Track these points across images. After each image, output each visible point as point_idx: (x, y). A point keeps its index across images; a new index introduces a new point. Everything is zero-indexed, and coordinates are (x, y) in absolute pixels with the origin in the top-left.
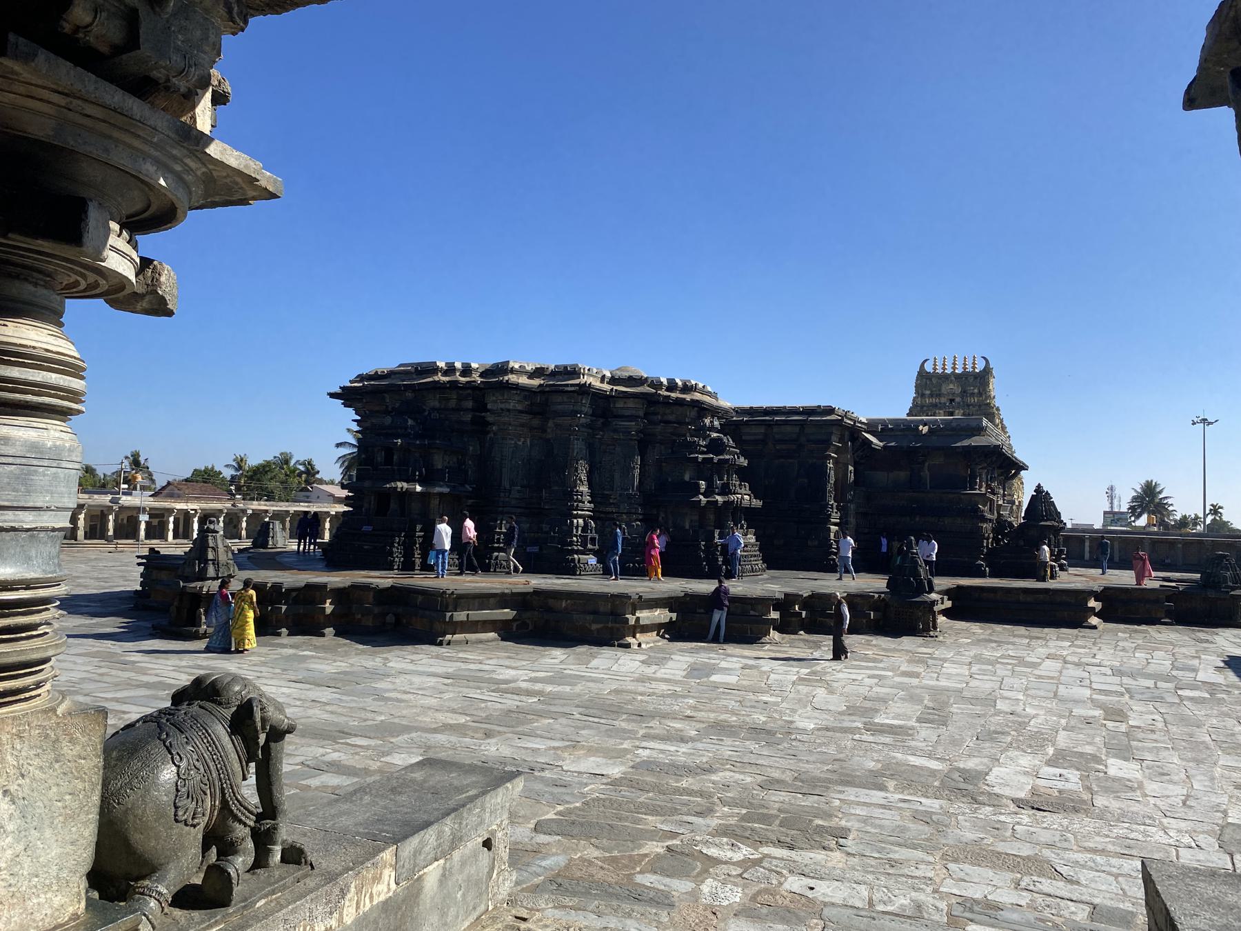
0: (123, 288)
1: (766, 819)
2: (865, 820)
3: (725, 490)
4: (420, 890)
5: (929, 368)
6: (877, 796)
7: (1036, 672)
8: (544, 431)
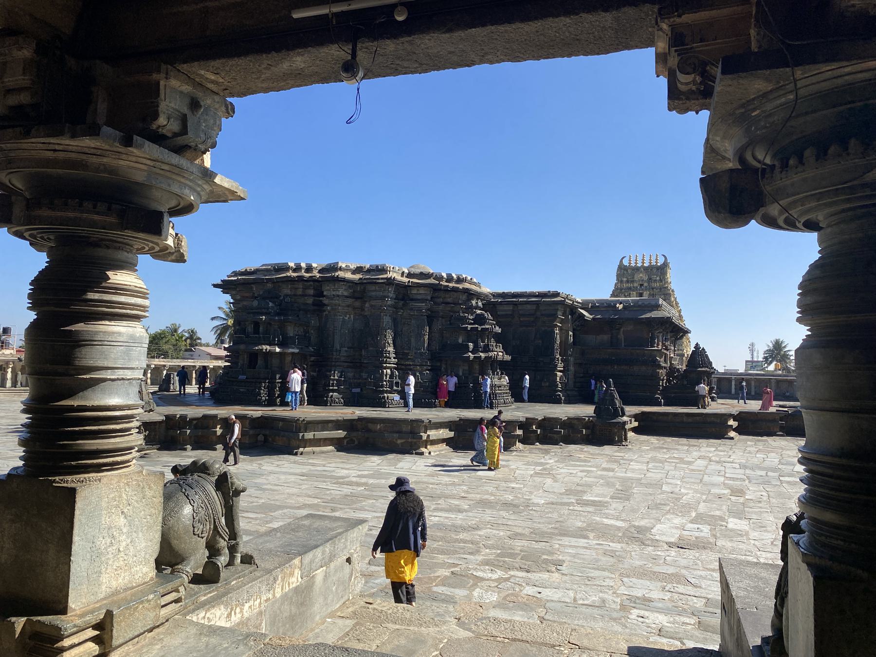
0: (167, 249)
1: (513, 556)
2: (574, 556)
3: (486, 349)
4: (313, 583)
5: (626, 263)
6: (582, 542)
8: (363, 310)
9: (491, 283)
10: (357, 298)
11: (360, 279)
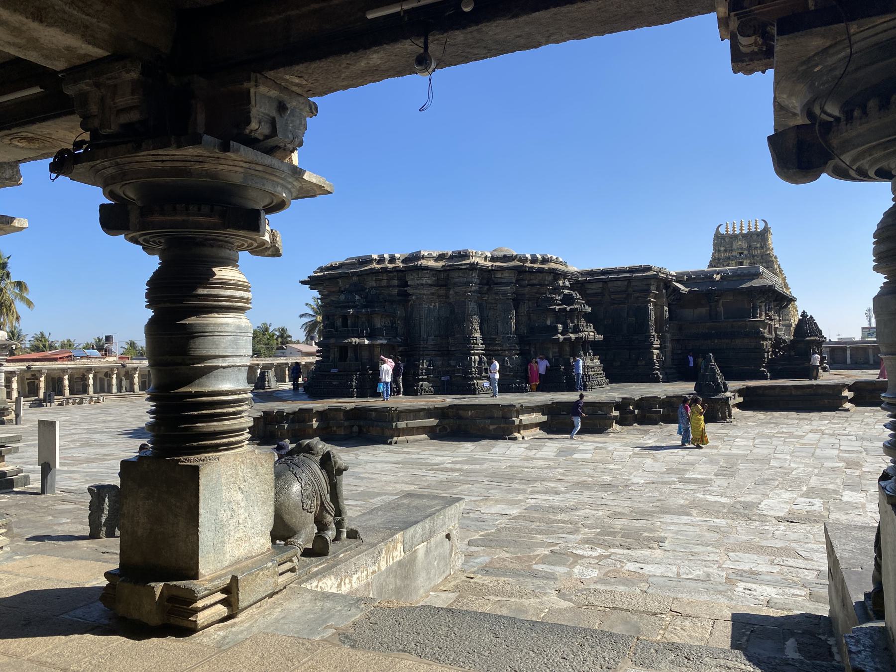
0: (264, 244)
1: (613, 534)
2: (676, 533)
3: (576, 330)
4: (416, 557)
5: (722, 231)
6: (685, 519)
7: (801, 441)
8: (447, 297)
9: (578, 262)
10: (441, 286)
11: (443, 266)
